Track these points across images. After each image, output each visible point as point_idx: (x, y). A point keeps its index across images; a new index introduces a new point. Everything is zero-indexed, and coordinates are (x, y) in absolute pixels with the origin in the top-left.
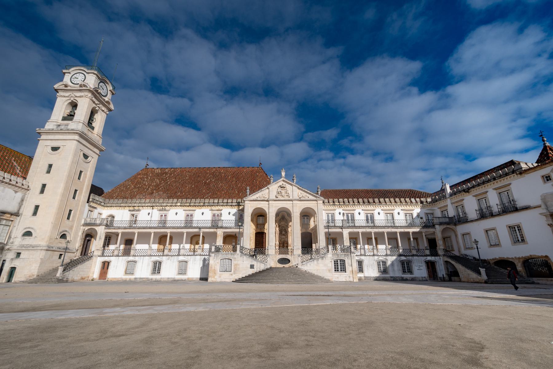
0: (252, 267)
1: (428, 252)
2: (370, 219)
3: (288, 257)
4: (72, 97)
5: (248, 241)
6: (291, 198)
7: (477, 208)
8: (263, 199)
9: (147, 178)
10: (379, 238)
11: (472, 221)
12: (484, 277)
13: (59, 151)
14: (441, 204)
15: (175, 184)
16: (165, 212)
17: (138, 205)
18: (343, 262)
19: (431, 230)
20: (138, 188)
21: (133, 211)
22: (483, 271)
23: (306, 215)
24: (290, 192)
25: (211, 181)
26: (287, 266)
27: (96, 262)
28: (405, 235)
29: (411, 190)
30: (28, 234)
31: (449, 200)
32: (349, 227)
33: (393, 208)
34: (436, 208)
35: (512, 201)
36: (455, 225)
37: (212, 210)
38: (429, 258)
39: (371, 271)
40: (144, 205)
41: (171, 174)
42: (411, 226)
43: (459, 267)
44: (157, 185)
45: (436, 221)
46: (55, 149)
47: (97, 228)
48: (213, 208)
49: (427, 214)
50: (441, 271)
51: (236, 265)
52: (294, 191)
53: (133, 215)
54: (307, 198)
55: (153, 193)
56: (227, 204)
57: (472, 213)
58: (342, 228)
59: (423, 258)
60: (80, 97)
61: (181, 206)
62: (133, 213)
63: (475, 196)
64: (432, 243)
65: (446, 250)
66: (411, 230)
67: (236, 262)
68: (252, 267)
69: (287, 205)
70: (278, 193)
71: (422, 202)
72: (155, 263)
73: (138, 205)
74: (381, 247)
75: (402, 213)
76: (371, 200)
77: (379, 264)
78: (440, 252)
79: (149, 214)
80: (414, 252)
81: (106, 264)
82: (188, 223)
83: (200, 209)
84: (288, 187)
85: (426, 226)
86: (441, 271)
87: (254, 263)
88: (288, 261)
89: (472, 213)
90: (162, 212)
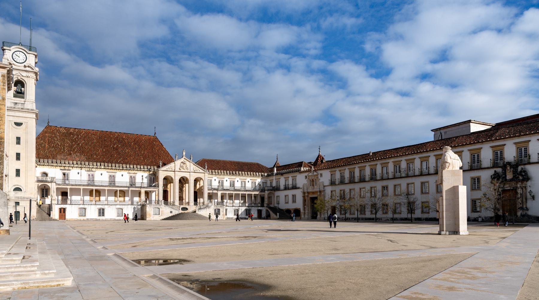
0: (171, 212)
1: (259, 205)
2: (232, 184)
3: (187, 207)
6: (189, 171)
7: (284, 184)
8: (171, 170)
9: (56, 137)
10: (237, 197)
12: (278, 217)
14: (271, 178)
15: (86, 147)
16: (92, 173)
17: (67, 165)
19: (263, 193)
20: (53, 147)
21: (65, 170)
22: (278, 214)
24: (188, 166)
26: (186, 212)
28: (250, 196)
29: (258, 164)
30: (18, 189)
32: (221, 190)
35: (296, 184)
36: (275, 191)
37: (130, 173)
38: (259, 208)
39: (231, 215)
40: (72, 166)
41: (78, 136)
42: (254, 190)
43: (271, 213)
44: (71, 147)
45: (266, 188)
47: (49, 184)
48: (130, 172)
49: (263, 183)
50: (264, 214)
52: (191, 166)
53: (64, 174)
54: (198, 171)
55: (71, 154)
57: (282, 187)
58: (217, 190)
59: (257, 208)
62: (64, 171)
64: (263, 199)
65: (268, 204)
66: (253, 193)
68: (171, 212)
69: (186, 175)
70: (181, 166)
71: (262, 175)
73: (67, 165)
74: (237, 202)
75: (250, 181)
76: (234, 172)
77: (235, 211)
78: (265, 205)
79: (78, 173)
80: (253, 205)
81: (62, 210)
82: (112, 182)
84: (188, 163)
85: (262, 190)
86: (264, 214)
87: (172, 210)
88: (187, 209)
89: (282, 187)
90: (89, 173)
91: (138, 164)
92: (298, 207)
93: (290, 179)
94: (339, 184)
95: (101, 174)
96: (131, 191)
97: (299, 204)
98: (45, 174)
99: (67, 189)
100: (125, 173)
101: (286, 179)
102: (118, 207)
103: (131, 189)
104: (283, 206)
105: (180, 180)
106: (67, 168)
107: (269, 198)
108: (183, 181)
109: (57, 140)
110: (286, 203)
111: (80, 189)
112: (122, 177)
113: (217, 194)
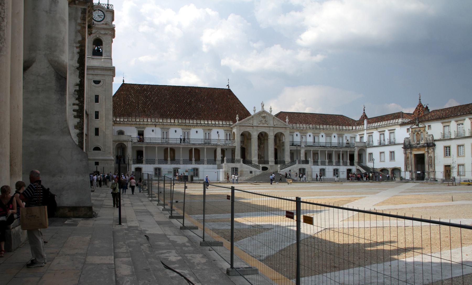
1: (348, 164)
5: (238, 155)
6: (269, 125)
8: (249, 125)
11: (375, 146)
18: (304, 169)
21: (140, 128)
23: (278, 137)
25: (190, 101)
31: (365, 131)
33: (331, 132)
34: (357, 134)
47: (125, 143)
51: (241, 171)
55: (144, 111)
56: (215, 126)
57: (376, 143)
61: (179, 125)
63: (380, 132)
67: (241, 169)
68: (251, 172)
78: (355, 164)
79: (153, 131)
83: (194, 128)
89: (376, 143)
91: (213, 120)
92: (398, 166)
93: (387, 134)
94: (454, 139)
96: (207, 148)
97: (399, 161)
98: (121, 133)
99: (142, 147)
100: (201, 131)
101: (382, 133)
102: (194, 166)
103: (206, 147)
104: (378, 165)
105: (258, 136)
106: (142, 126)
107: (360, 156)
108: (262, 137)
110: (381, 161)
111: (155, 147)
112: (197, 135)
113: (300, 150)
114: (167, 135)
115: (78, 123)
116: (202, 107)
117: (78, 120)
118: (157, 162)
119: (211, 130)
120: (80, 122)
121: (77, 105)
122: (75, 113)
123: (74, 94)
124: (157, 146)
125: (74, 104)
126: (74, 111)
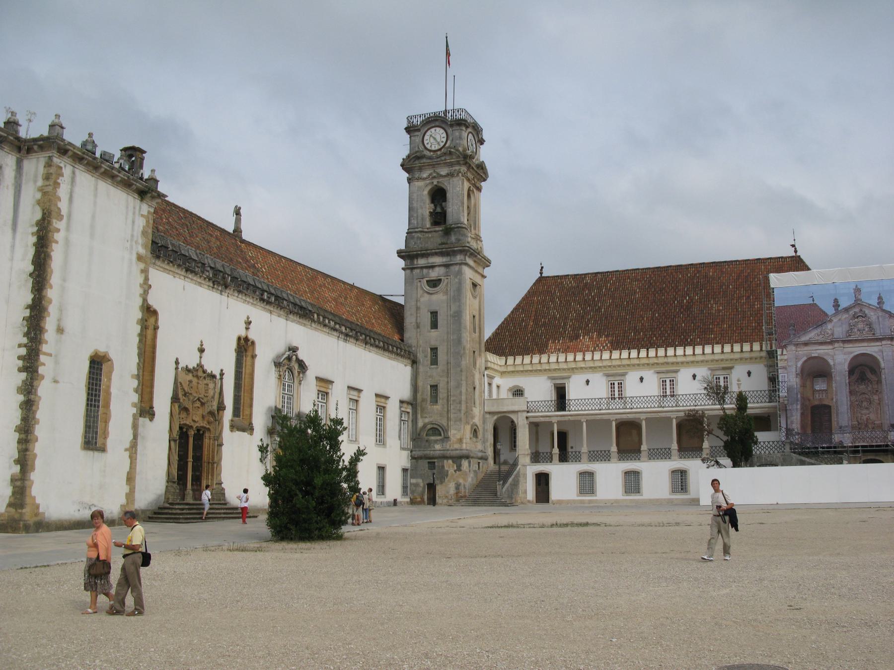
4: (434, 177)
9: (553, 301)
13: (442, 286)
20: (544, 325)
25: (691, 299)
27: (525, 475)
41: (600, 289)
46: (434, 283)
55: (577, 337)
60: (450, 175)
72: (627, 473)
90: (612, 378)
95: (642, 379)
98: (518, 392)
99: (551, 424)
109: (555, 308)
111: (580, 423)
114: (620, 391)
115: (23, 381)
116: (719, 311)
117: (24, 375)
118: (585, 457)
119: (731, 368)
120: (27, 379)
121: (25, 346)
122: (20, 363)
123: (22, 325)
124: (583, 419)
125: (20, 346)
126: (19, 358)
